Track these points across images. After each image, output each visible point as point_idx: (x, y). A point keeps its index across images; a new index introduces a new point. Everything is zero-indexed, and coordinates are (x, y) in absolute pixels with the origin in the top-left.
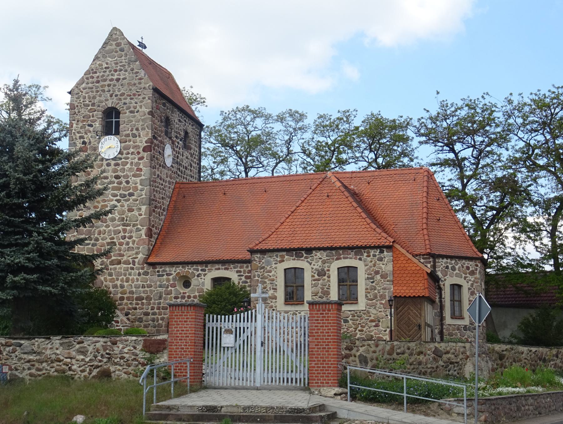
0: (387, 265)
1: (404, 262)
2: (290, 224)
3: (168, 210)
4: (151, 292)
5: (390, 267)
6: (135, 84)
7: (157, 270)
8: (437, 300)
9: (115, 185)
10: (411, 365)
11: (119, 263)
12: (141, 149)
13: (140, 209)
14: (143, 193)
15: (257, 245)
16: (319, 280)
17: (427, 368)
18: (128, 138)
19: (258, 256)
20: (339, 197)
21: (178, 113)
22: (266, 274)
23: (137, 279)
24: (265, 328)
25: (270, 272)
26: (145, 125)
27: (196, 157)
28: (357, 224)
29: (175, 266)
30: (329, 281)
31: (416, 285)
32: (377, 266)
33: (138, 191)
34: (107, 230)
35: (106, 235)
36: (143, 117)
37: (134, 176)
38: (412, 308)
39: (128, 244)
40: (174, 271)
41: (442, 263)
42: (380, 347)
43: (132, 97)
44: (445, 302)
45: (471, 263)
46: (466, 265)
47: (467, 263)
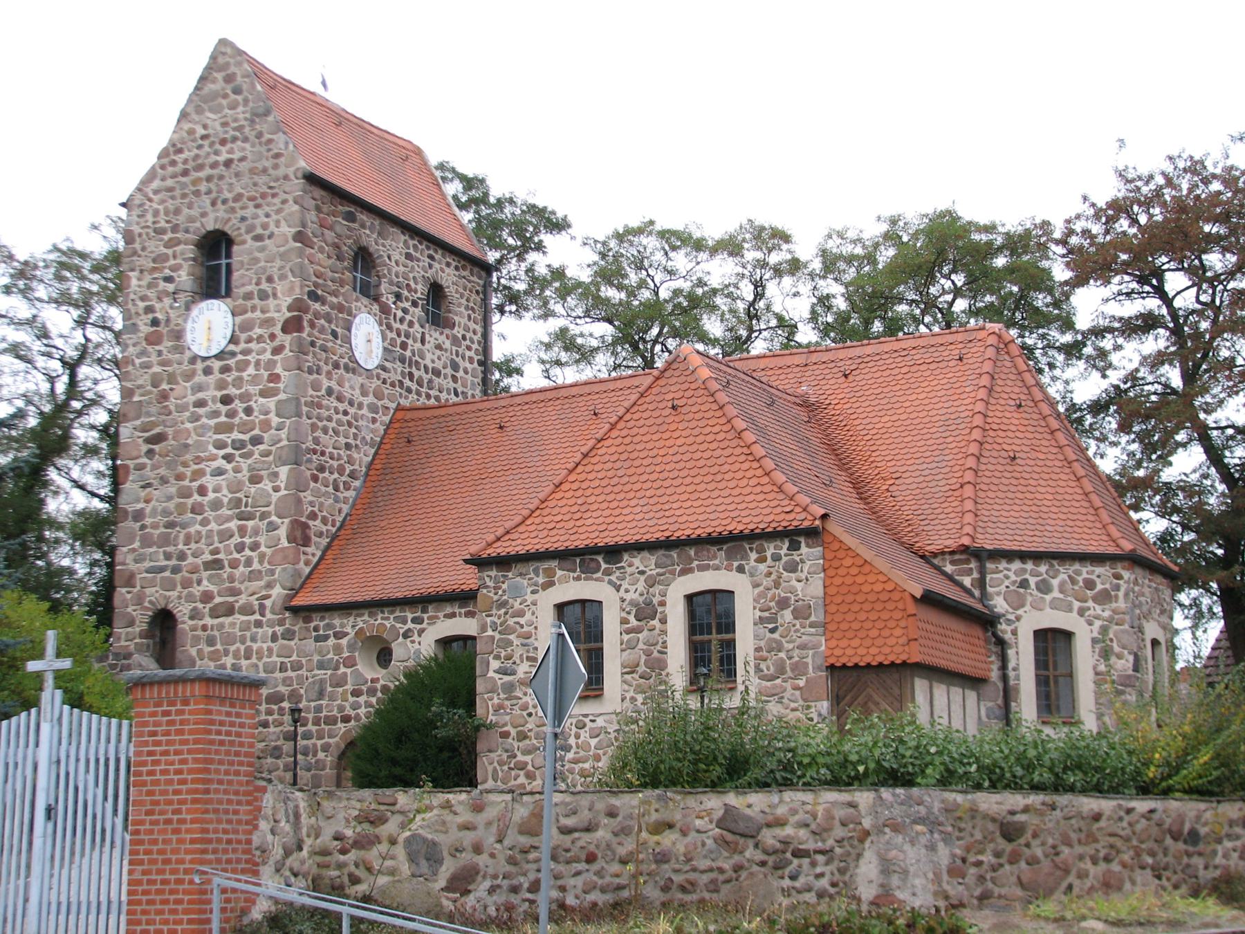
0: (808, 585)
1: (854, 571)
2: (574, 486)
3: (367, 475)
4: (300, 680)
5: (816, 588)
6: (265, 170)
7: (312, 625)
8: (994, 675)
9: (223, 419)
10: (624, 862)
11: (230, 611)
12: (279, 326)
13: (276, 475)
14: (283, 434)
15: (489, 545)
16: (637, 630)
17: (694, 870)
18: (249, 304)
19: (493, 573)
20: (703, 408)
21: (403, 238)
22: (511, 622)
23: (270, 650)
24: (58, 762)
25: (521, 614)
26: (287, 268)
27: (475, 346)
28: (740, 475)
29: (355, 612)
30: (664, 632)
31: (886, 633)
32: (784, 584)
33: (273, 431)
34: (204, 530)
35: (202, 545)
36: (282, 249)
37: (264, 394)
38: (875, 696)
39: (249, 562)
40: (350, 625)
41: (1003, 577)
42: (490, 813)
43: (259, 201)
44: (1017, 678)
45: (1099, 570)
46: (1085, 575)
47: (1086, 571)
